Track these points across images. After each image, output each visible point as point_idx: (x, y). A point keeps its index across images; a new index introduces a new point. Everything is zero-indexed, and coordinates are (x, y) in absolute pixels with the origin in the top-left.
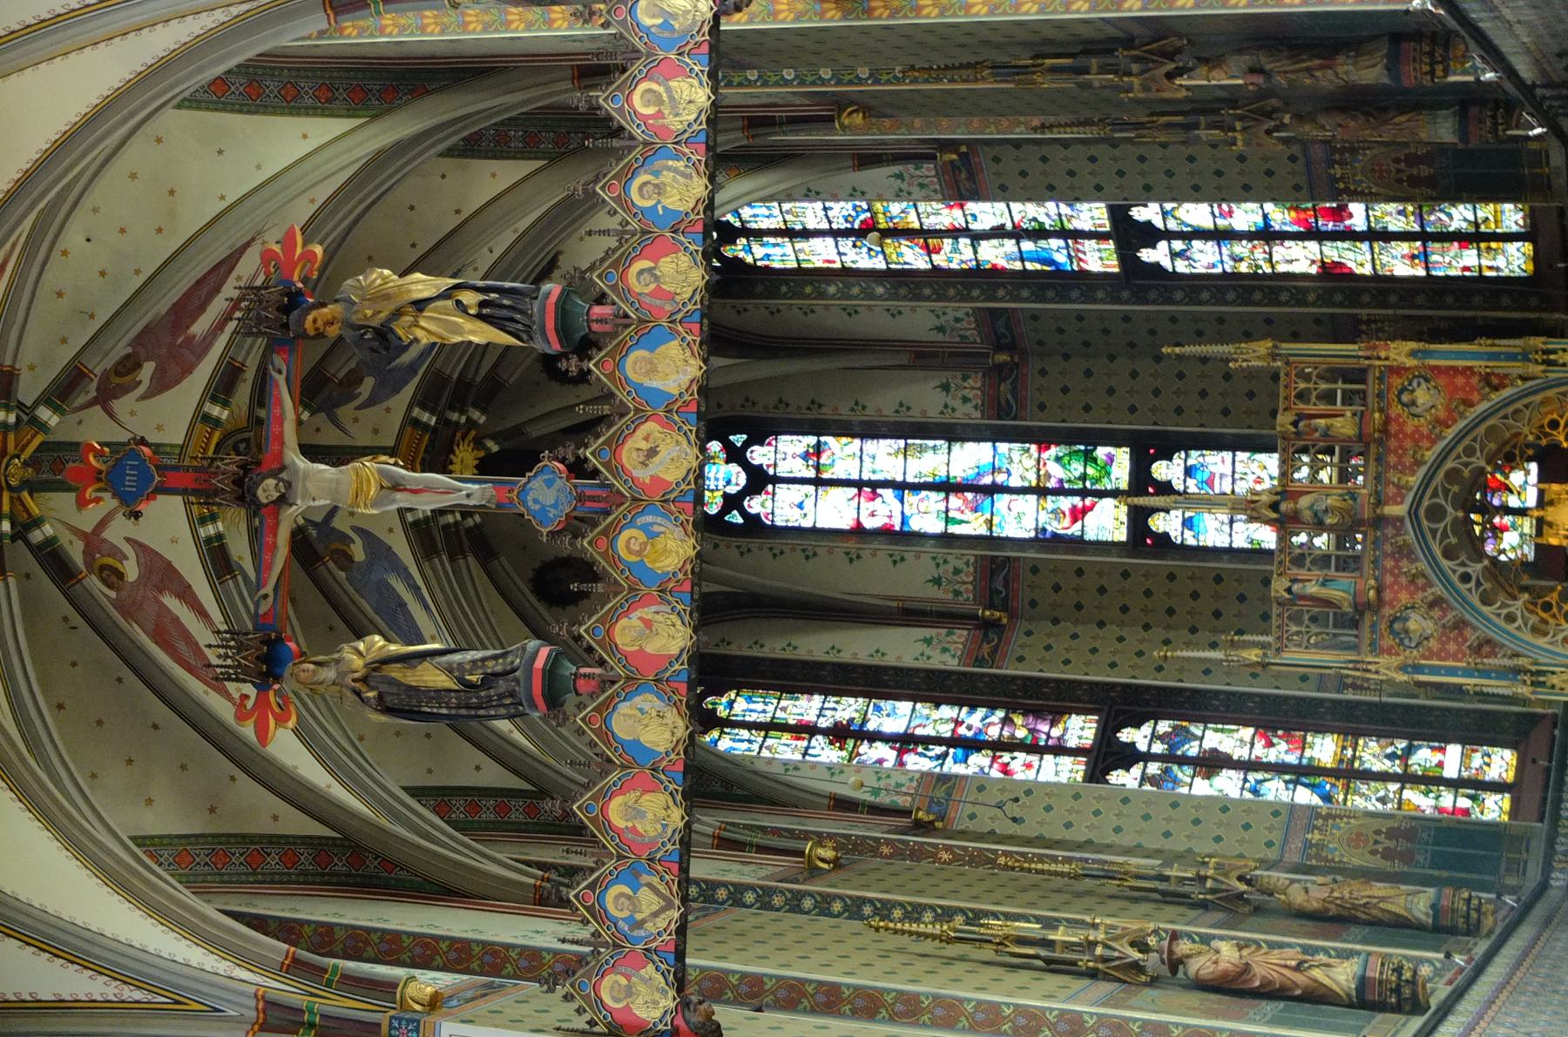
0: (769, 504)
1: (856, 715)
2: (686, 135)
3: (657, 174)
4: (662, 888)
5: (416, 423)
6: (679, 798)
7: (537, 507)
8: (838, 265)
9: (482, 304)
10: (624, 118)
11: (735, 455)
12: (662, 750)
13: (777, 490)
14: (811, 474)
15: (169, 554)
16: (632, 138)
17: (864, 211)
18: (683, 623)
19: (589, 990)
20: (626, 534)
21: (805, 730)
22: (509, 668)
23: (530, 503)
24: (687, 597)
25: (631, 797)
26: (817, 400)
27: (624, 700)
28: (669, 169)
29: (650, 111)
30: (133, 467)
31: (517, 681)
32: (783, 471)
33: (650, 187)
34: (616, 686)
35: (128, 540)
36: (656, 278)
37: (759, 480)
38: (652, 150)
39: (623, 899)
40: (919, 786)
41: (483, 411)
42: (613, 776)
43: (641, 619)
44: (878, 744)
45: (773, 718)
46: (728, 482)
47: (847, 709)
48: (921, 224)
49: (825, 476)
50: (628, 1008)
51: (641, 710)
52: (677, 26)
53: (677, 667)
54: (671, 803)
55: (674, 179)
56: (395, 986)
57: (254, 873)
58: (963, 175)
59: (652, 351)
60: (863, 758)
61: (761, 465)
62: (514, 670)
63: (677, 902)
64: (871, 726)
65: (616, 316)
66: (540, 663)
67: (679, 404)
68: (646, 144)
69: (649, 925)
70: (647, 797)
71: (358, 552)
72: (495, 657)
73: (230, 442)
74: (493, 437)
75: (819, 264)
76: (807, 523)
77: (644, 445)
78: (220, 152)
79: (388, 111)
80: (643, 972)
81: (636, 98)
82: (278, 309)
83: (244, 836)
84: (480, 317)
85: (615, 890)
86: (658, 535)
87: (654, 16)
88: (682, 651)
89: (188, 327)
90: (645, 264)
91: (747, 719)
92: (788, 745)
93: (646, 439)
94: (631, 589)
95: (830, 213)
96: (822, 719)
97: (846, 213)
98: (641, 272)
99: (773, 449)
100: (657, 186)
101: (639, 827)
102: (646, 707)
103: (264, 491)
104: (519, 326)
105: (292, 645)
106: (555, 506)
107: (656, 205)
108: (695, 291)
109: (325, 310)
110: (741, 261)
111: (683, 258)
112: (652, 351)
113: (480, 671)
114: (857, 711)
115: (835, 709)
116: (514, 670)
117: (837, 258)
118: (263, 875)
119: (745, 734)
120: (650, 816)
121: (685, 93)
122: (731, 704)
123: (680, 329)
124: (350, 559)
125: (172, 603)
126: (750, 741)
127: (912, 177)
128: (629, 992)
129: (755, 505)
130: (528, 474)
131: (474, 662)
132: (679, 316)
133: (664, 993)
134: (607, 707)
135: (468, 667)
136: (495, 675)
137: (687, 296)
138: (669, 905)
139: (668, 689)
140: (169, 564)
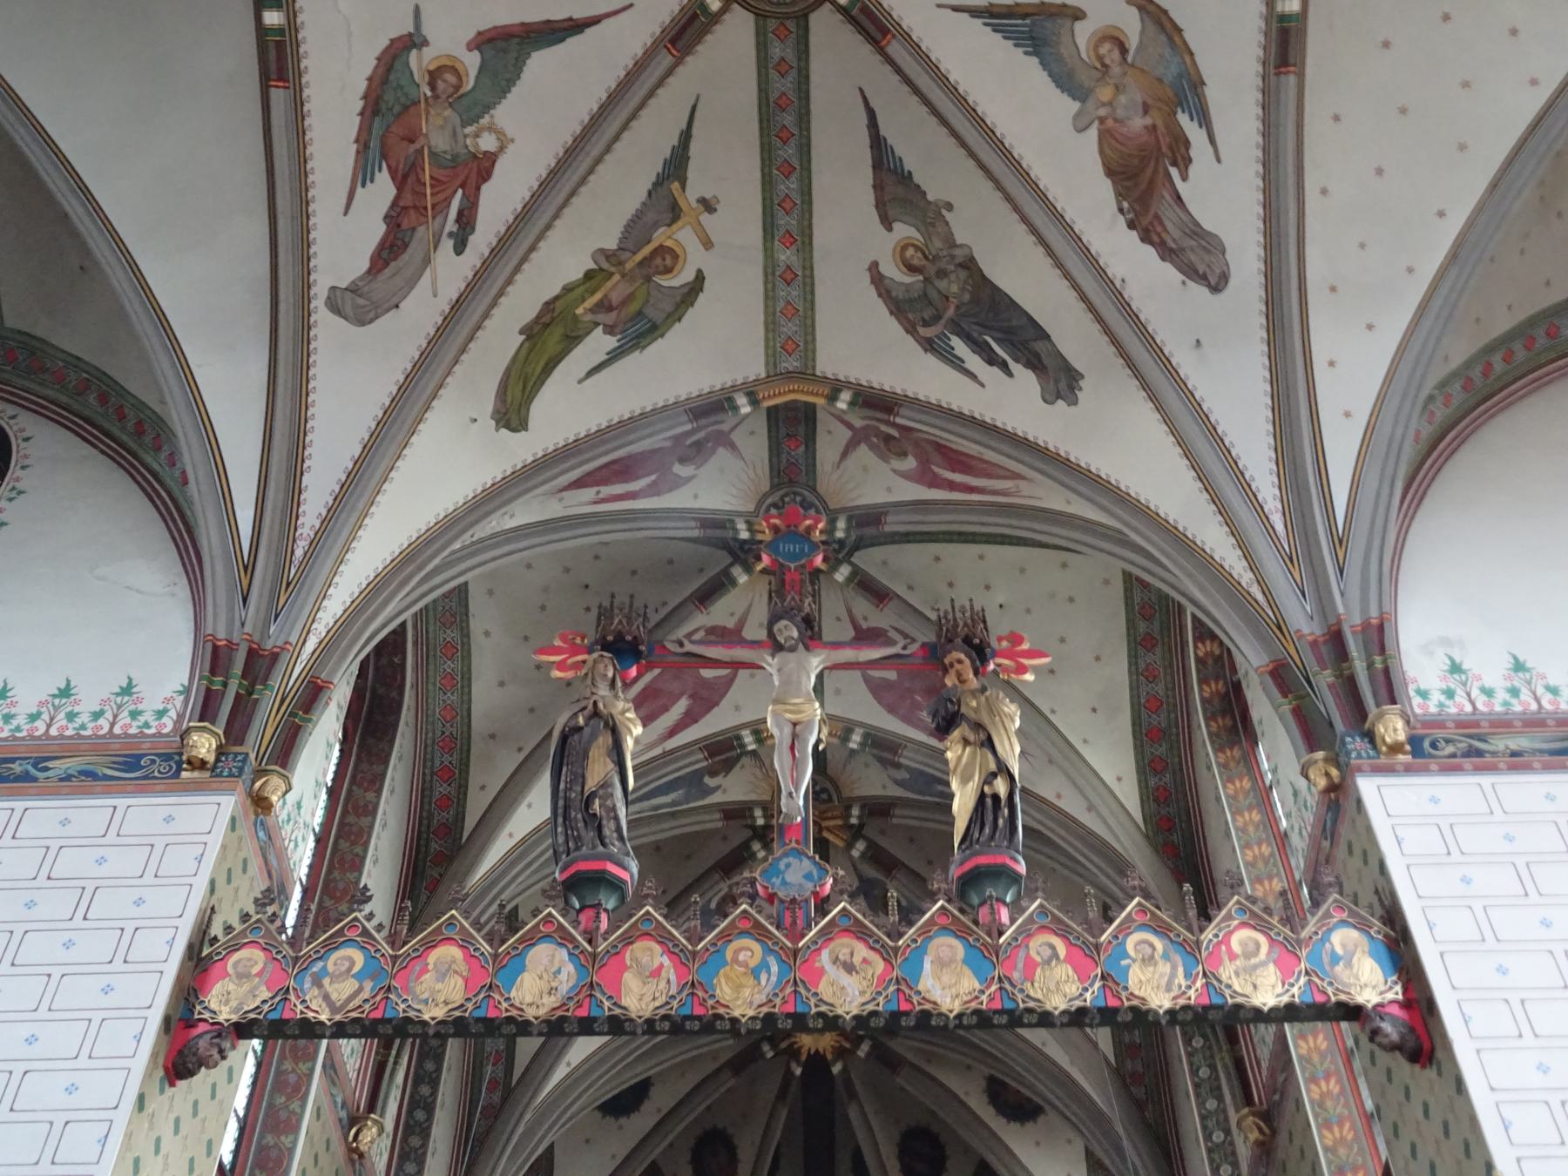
2: (1215, 983)
3: (1166, 957)
4: (357, 1002)
6: (457, 1013)
7: (782, 866)
9: (996, 797)
10: (1223, 920)
12: (513, 994)
15: (726, 703)
16: (1202, 930)
18: (657, 1008)
19: (251, 938)
20: (757, 947)
22: (607, 841)
23: (785, 860)
24: (686, 1011)
25: (462, 967)
27: (570, 954)
28: (1174, 968)
29: (1235, 945)
30: (802, 550)
31: (594, 847)
33: (1149, 950)
34: (585, 944)
36: (1048, 962)
38: (1191, 950)
39: (347, 964)
41: (868, 1055)
42: (486, 948)
43: (661, 966)
50: (226, 974)
51: (559, 971)
52: (1339, 968)
53: (607, 1004)
54: (450, 1007)
55: (1162, 975)
56: (284, 766)
57: (432, 773)
59: (965, 961)
62: (604, 844)
63: (338, 1017)
65: (1001, 925)
66: (612, 868)
67: (907, 991)
68: (1198, 943)
69: (316, 991)
70: (460, 982)
72: (619, 829)
73: (828, 785)
74: (845, 1070)
77: (857, 960)
78: (1094, 710)
79: (1156, 850)
80: (264, 988)
81: (1246, 933)
82: (967, 636)
83: (467, 765)
84: (982, 796)
85: (359, 958)
86: (757, 978)
87: (1344, 946)
88: (625, 1008)
90: (1062, 950)
93: (865, 961)
94: (694, 954)
98: (1053, 947)
100: (1152, 957)
101: (427, 976)
102: (563, 976)
103: (786, 627)
104: (976, 835)
105: (633, 671)
106: (784, 883)
107: (1128, 957)
108: (1039, 1001)
109: (971, 676)
111: (1074, 988)
112: (965, 961)
113: (604, 814)
116: (604, 844)
118: (431, 781)
120: (439, 986)
121: (1265, 981)
123: (994, 988)
125: (681, 706)
128: (243, 976)
130: (817, 857)
131: (614, 809)
132: (1007, 986)
133: (235, 1011)
134: (564, 938)
135: (609, 803)
136: (600, 828)
137: (1032, 993)
138: (334, 1009)
139: (581, 997)
140: (716, 704)
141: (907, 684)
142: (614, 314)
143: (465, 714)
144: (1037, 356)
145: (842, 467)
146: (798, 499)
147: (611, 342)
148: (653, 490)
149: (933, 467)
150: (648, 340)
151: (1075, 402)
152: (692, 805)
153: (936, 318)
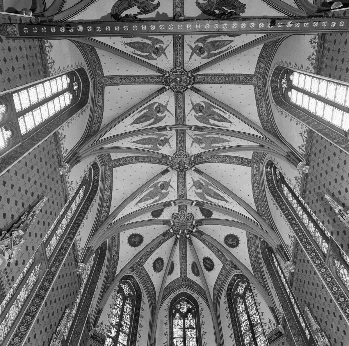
0: (178, 318)
1: (124, 331)
5: (192, 202)
8: (240, 323)
11: (189, 311)
13: (181, 320)
14: (186, 327)
17: (257, 323)
21: (121, 317)
26: (205, 324)
32: (187, 321)
35: (165, 115)
37: (184, 316)
40: (102, 334)
41: (196, 231)
44: (116, 333)
45: (125, 312)
46: (183, 310)
47: (126, 329)
48: (257, 337)
49: (186, 330)
58: (275, 337)
60: (112, 329)
61: (187, 316)
64: (121, 333)
71: (164, 191)
73: (186, 154)
75: (240, 319)
76: (174, 326)
89: (210, 118)
91: (125, 306)
92: (118, 312)
95: (254, 316)
96: (123, 322)
97: (255, 319)
99: (191, 318)
110: (237, 302)
114: (125, 331)
115: (126, 326)
117: (242, 322)
119: (121, 304)
122: (129, 304)
124: (163, 189)
126: (119, 305)
127: (271, 324)
129: (177, 315)
141: (205, 115)
142: (140, 4)
143: (102, 114)
144: (235, 6)
145: (190, 61)
146: (180, 71)
147: (139, 10)
148: (146, 57)
149: (211, 52)
150: (147, 13)
151: (246, 5)
152: (154, 151)
153: (212, 7)
